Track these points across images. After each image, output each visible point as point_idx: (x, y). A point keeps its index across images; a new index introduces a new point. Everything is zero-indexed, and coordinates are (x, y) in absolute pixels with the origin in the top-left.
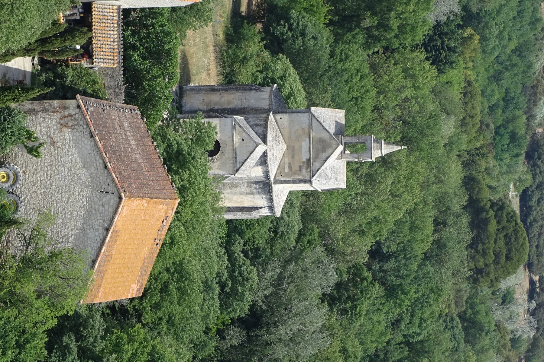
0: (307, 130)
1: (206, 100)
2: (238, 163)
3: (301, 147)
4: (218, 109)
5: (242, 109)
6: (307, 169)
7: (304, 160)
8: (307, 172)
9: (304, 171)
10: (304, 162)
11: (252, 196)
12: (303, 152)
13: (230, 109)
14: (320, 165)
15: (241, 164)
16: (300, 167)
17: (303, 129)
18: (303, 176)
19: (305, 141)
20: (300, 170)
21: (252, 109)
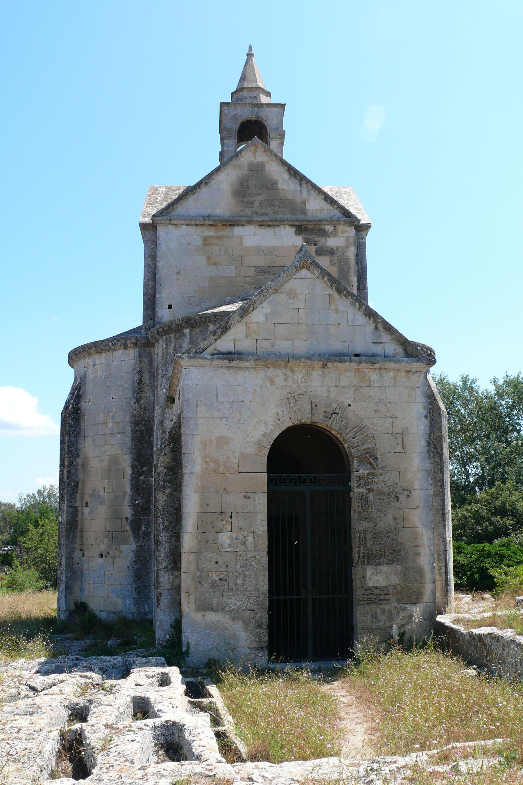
0: (210, 232)
1: (103, 547)
2: (377, 349)
3: (259, 250)
4: (134, 506)
5: (134, 432)
6: (324, 234)
7: (299, 241)
8: (335, 234)
9: (332, 242)
12: (275, 243)
13: (133, 467)
14: (313, 193)
15: (385, 337)
17: (206, 241)
18: (348, 246)
19: (241, 238)
20: (331, 252)
21: (138, 400)
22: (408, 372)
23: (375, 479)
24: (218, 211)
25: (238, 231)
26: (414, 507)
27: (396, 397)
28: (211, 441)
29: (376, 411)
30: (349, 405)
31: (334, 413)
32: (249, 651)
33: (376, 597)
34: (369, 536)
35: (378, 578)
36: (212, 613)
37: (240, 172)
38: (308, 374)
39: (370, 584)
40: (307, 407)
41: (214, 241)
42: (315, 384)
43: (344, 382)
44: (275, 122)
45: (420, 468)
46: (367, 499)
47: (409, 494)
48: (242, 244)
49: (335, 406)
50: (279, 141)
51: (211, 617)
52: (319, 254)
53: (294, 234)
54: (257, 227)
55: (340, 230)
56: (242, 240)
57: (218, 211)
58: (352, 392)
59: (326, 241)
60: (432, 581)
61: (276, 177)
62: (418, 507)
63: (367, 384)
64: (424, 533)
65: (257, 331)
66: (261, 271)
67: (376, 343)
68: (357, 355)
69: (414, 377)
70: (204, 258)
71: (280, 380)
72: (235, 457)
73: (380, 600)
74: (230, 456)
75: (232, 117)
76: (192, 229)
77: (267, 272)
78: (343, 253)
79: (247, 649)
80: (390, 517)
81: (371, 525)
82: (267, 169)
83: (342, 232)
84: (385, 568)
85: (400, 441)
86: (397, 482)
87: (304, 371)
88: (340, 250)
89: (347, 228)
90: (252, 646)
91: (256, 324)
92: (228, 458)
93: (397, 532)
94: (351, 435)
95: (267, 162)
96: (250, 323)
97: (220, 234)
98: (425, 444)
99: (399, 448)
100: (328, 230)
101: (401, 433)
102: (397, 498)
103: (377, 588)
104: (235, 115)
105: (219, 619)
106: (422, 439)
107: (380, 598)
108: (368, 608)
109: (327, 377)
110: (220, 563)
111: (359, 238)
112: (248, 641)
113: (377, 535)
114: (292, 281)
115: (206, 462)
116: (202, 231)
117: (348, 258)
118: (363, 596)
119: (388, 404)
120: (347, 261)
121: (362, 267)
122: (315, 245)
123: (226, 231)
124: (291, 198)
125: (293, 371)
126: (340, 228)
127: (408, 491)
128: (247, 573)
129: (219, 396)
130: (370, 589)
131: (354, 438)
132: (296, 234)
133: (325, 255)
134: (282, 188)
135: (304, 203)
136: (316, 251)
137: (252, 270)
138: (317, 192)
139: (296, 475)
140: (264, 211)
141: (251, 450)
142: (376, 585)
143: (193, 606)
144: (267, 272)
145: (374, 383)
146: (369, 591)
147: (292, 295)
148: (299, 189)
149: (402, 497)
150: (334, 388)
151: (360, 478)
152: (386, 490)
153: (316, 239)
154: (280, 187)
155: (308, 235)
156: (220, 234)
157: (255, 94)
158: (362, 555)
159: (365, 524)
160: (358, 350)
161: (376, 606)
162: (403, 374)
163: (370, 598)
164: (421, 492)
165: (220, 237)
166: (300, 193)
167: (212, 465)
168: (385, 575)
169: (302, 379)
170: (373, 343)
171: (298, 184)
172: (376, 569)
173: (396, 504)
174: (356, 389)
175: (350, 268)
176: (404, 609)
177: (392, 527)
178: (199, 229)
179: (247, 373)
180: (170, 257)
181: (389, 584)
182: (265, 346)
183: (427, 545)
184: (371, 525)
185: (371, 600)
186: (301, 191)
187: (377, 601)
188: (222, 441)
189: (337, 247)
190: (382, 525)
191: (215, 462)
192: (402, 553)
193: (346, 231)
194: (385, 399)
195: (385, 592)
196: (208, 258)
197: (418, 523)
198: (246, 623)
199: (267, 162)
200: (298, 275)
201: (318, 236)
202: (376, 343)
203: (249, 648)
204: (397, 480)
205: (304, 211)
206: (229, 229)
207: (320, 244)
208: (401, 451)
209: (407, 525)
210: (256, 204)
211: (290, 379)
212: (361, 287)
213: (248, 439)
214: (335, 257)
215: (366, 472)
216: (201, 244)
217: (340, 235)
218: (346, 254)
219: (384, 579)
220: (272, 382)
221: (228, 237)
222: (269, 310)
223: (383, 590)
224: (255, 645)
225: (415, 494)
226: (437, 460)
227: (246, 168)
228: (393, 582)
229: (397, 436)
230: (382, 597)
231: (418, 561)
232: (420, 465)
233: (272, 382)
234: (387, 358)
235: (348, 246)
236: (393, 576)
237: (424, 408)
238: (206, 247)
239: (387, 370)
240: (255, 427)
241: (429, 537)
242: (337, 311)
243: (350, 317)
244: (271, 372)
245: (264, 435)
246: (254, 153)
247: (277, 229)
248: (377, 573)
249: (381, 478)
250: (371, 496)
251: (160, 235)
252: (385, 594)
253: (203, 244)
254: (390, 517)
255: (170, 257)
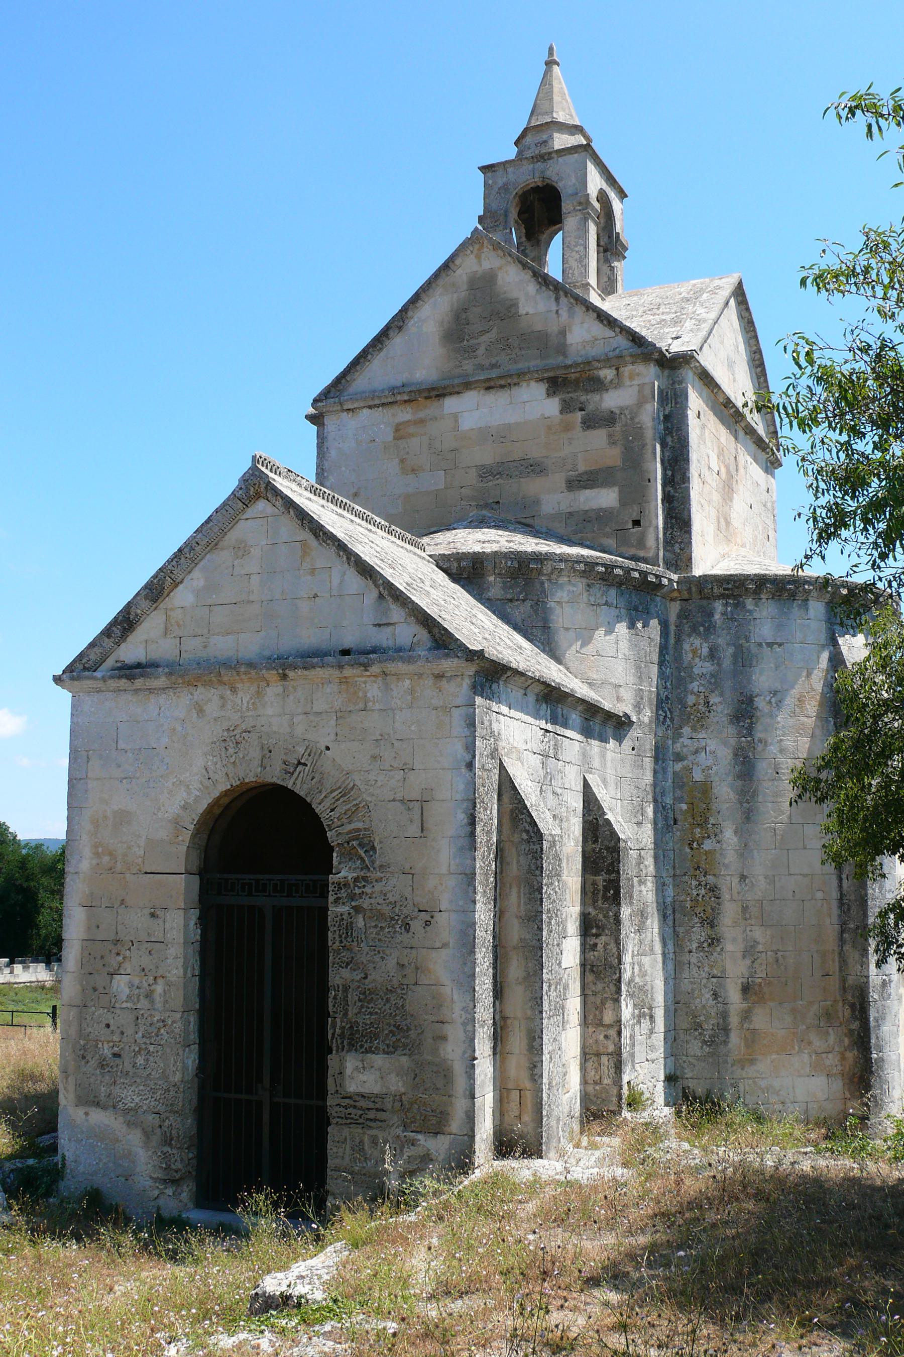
0: (404, 414)
2: (382, 638)
3: (485, 434)
6: (598, 385)
7: (552, 407)
8: (617, 383)
9: (612, 400)
10: (566, 407)
11: (761, 703)
12: (512, 417)
14: (579, 310)
15: (397, 613)
16: (589, 423)
17: (400, 433)
18: (641, 402)
19: (455, 417)
20: (609, 419)
22: (439, 677)
23: (368, 890)
24: (418, 375)
25: (451, 404)
26: (438, 945)
27: (413, 728)
28: (105, 817)
29: (374, 757)
30: (328, 748)
31: (299, 763)
32: (150, 1183)
33: (361, 1112)
34: (353, 996)
35: (365, 1078)
36: (99, 1110)
37: (455, 295)
38: (259, 694)
39: (352, 1087)
40: (255, 754)
41: (411, 430)
42: (269, 711)
43: (320, 705)
44: (574, 180)
45: (453, 868)
46: (350, 927)
47: (429, 919)
48: (456, 428)
49: (301, 750)
50: (579, 216)
51: (99, 1117)
52: (588, 427)
53: (545, 395)
54: (482, 392)
55: (626, 374)
56: (456, 421)
57: (418, 375)
58: (333, 722)
59: (601, 399)
60: (468, 1093)
61: (514, 294)
62: (445, 945)
63: (361, 705)
64: (455, 997)
65: (181, 623)
66: (488, 473)
67: (380, 625)
68: (346, 652)
69: (450, 687)
70: (396, 461)
71: (212, 709)
72: (139, 847)
73: (367, 1119)
74: (132, 843)
75: (499, 189)
76: (378, 413)
77: (498, 474)
78: (632, 419)
79: (148, 1178)
80: (391, 962)
81: (358, 975)
82: (500, 281)
83: (631, 378)
84: (378, 1060)
85: (417, 816)
86: (407, 895)
87: (253, 689)
88: (627, 412)
89: (640, 368)
90: (155, 1176)
91: (180, 611)
92: (129, 848)
93: (404, 992)
94: (327, 803)
95: (500, 268)
96: (172, 609)
97: (421, 415)
98: (466, 821)
99: (414, 830)
100: (606, 378)
101: (419, 799)
102: (407, 927)
103: (363, 1096)
104: (505, 184)
105: (107, 1122)
106: (459, 811)
107: (368, 1117)
108: (346, 1132)
109: (291, 697)
110: (112, 1028)
111: (674, 383)
112: (150, 1166)
113: (367, 996)
114: (242, 524)
115: (97, 855)
116: (393, 415)
117: (641, 427)
118: (337, 1109)
119: (396, 744)
120: (639, 432)
121: (679, 439)
122: (581, 409)
123: (431, 409)
124: (539, 327)
125: (234, 690)
126: (627, 370)
127: (429, 915)
128: (151, 1048)
129: (120, 742)
130: (350, 1098)
131: (332, 810)
132: (548, 395)
133: (599, 427)
134: (524, 312)
135: (563, 333)
136: (584, 422)
137: (473, 473)
138: (584, 309)
139: (251, 876)
140: (494, 361)
141: (163, 834)
142: (362, 1090)
143: (72, 1096)
144: (498, 474)
145: (374, 702)
146: (347, 1101)
147: (242, 550)
148: (554, 308)
149: (416, 926)
150: (301, 717)
151: (339, 886)
152: (386, 909)
153: (583, 398)
154: (522, 311)
155: (568, 393)
156: (421, 415)
157: (545, 137)
158: (338, 1031)
159: (346, 973)
160: (348, 641)
161: (360, 1131)
162: (429, 682)
163: (350, 1114)
164: (454, 916)
165: (422, 421)
166: (555, 316)
167: (106, 859)
168: (378, 1073)
169: (248, 703)
170: (375, 625)
171: (553, 299)
172: (362, 1061)
173: (404, 938)
174: (340, 714)
175: (644, 446)
176: (413, 1143)
177: (395, 983)
178: (388, 412)
179: (162, 699)
180: (343, 469)
181: (384, 1091)
182: (193, 648)
183: (460, 1021)
184: (358, 975)
185: (352, 1118)
186: (557, 311)
187: (361, 1121)
188: (123, 818)
189: (622, 409)
190: (377, 977)
191: (111, 854)
192: (413, 1034)
193: (638, 374)
194: (392, 732)
195: (377, 1106)
196: (402, 461)
197: (444, 977)
198: (147, 1134)
199: (500, 268)
200: (249, 513)
201: (587, 391)
202: (380, 625)
203: (151, 1177)
204: (407, 892)
205: (562, 349)
206: (435, 403)
207: (590, 407)
208: (418, 834)
209: (424, 980)
210: (481, 350)
211: (229, 705)
212: (678, 478)
213: (160, 815)
214: (618, 427)
215: (351, 876)
216: (391, 438)
217: (628, 383)
218: (637, 420)
219: (376, 1082)
220: (201, 711)
221: (435, 419)
222: (202, 583)
223: (374, 1102)
224: (159, 1174)
225: (441, 919)
226: (535, 847)
227: (465, 287)
228: (393, 1089)
229: (411, 805)
230: (371, 1115)
231: (442, 1052)
232: (452, 862)
233: (201, 711)
234: (401, 653)
235: (641, 402)
236: (393, 1075)
237: (467, 749)
238: (399, 442)
239: (398, 676)
240: (170, 792)
241: (464, 1005)
242: (313, 571)
243: (336, 580)
244: (200, 693)
245: (184, 808)
246: (478, 257)
247: (515, 390)
248: (364, 1068)
249: (378, 887)
250: (360, 922)
251: (328, 432)
252: (377, 1110)
253: (395, 438)
254: (391, 962)
255: (343, 469)
